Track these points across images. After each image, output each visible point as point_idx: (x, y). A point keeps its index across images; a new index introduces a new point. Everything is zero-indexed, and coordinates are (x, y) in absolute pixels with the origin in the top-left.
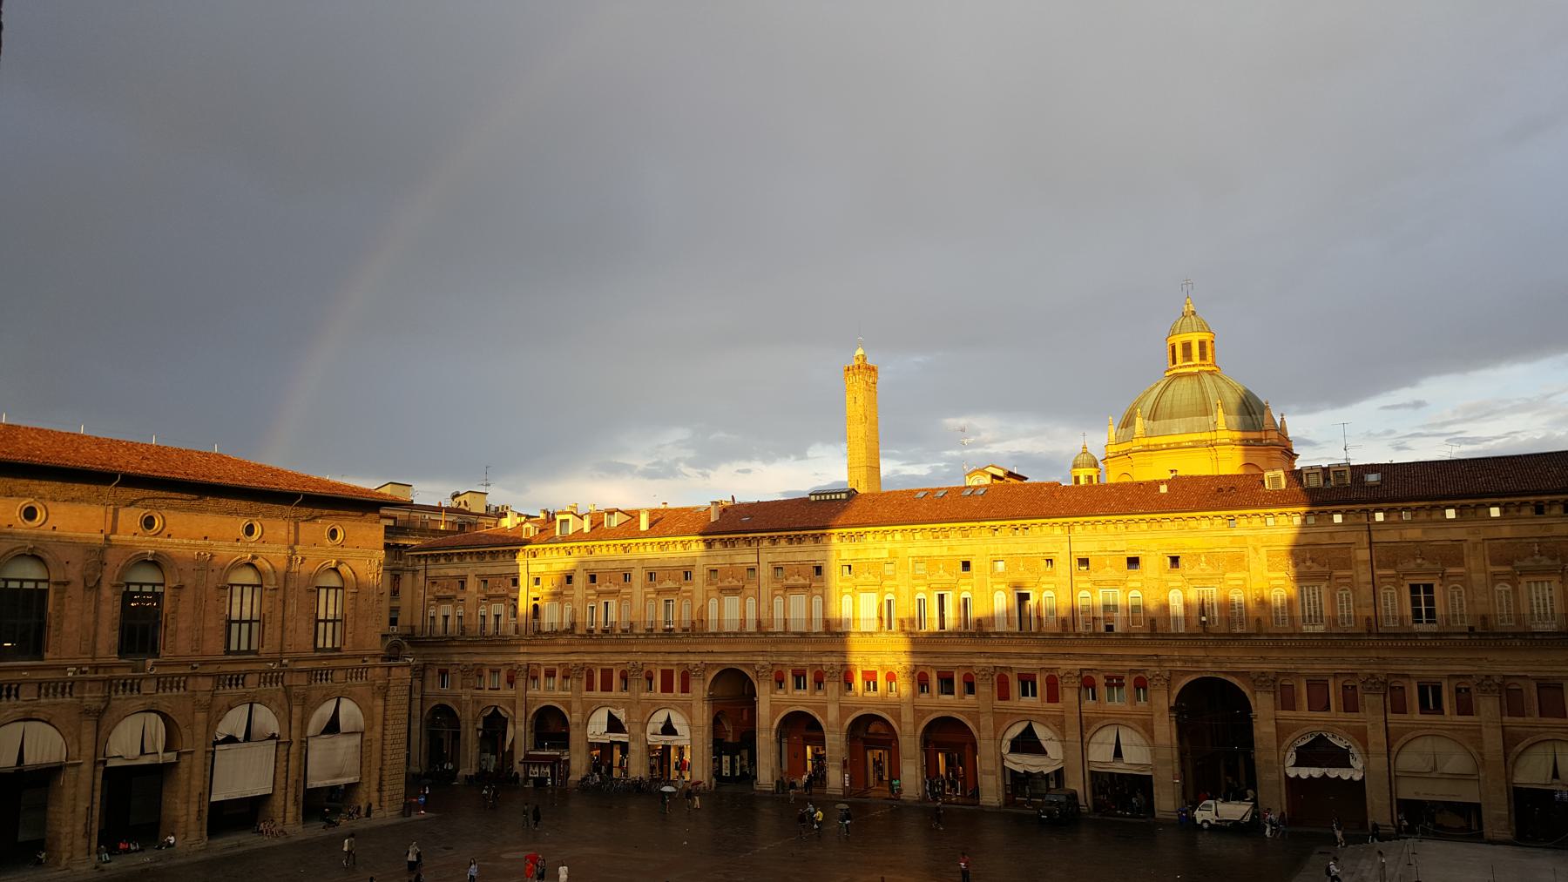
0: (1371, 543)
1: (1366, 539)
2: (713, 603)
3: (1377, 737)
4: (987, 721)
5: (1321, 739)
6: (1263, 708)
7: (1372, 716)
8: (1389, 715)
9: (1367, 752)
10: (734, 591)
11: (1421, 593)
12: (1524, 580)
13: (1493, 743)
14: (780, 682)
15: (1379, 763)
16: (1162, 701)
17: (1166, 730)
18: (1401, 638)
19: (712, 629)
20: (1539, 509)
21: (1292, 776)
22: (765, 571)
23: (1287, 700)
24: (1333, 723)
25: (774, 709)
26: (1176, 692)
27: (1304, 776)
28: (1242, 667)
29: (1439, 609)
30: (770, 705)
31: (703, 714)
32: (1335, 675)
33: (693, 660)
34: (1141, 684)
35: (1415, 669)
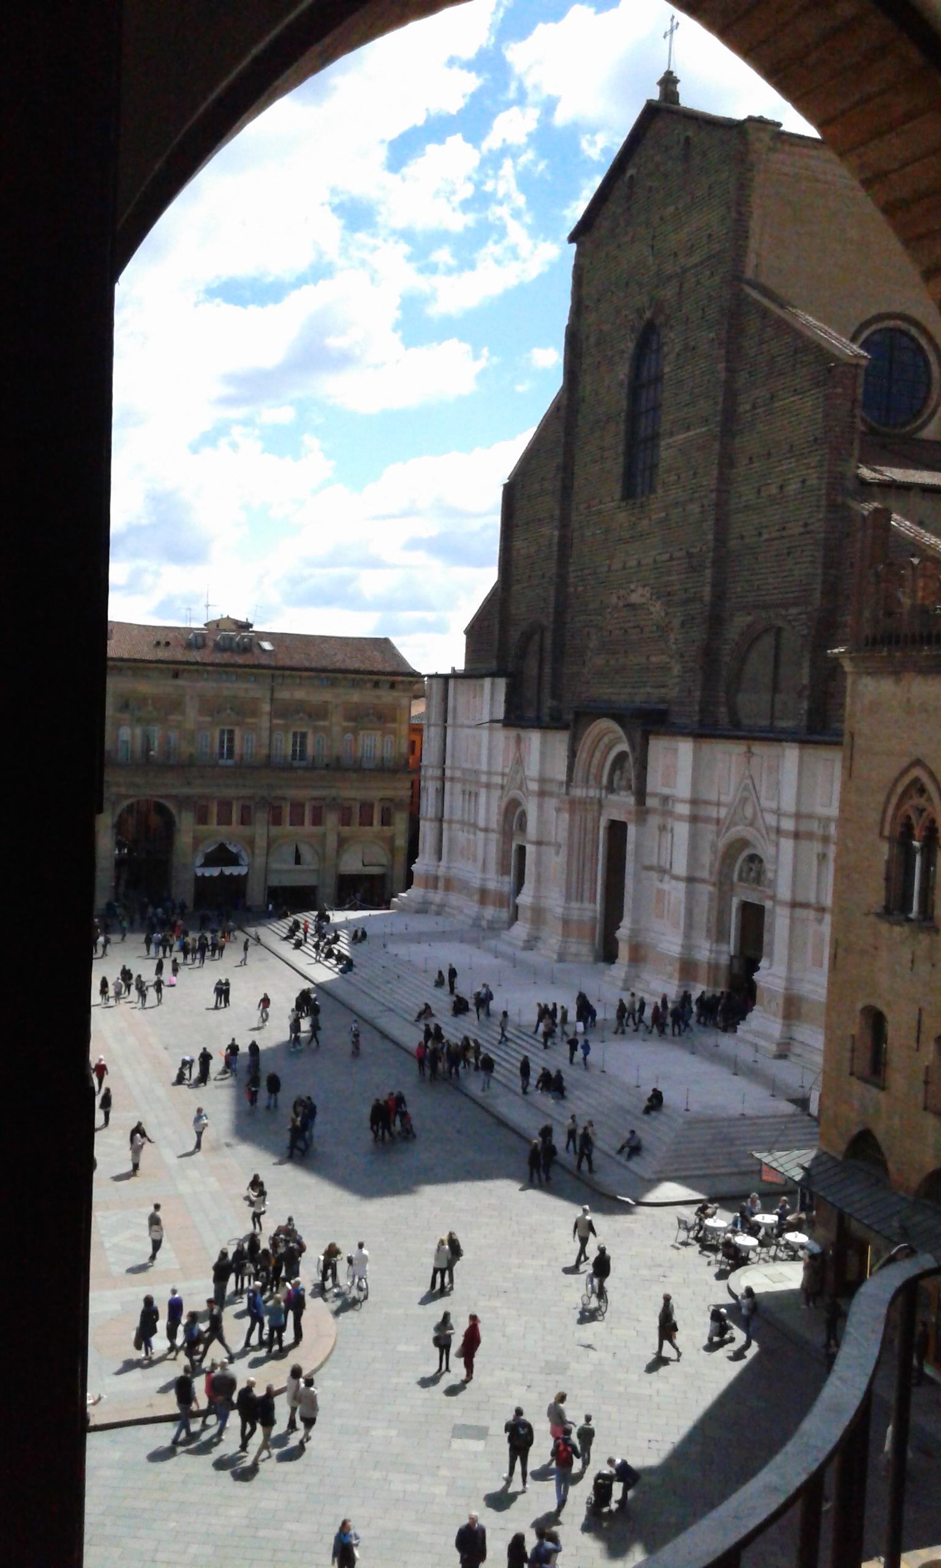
0: (272, 700)
1: (268, 695)
3: (261, 843)
5: (222, 847)
7: (260, 830)
8: (271, 827)
9: (253, 852)
12: (361, 733)
13: (332, 841)
15: (260, 861)
20: (376, 685)
21: (199, 874)
23: (202, 819)
24: (230, 834)
26: (118, 811)
27: (207, 874)
28: (174, 792)
29: (310, 750)
32: (238, 798)
35: (293, 793)
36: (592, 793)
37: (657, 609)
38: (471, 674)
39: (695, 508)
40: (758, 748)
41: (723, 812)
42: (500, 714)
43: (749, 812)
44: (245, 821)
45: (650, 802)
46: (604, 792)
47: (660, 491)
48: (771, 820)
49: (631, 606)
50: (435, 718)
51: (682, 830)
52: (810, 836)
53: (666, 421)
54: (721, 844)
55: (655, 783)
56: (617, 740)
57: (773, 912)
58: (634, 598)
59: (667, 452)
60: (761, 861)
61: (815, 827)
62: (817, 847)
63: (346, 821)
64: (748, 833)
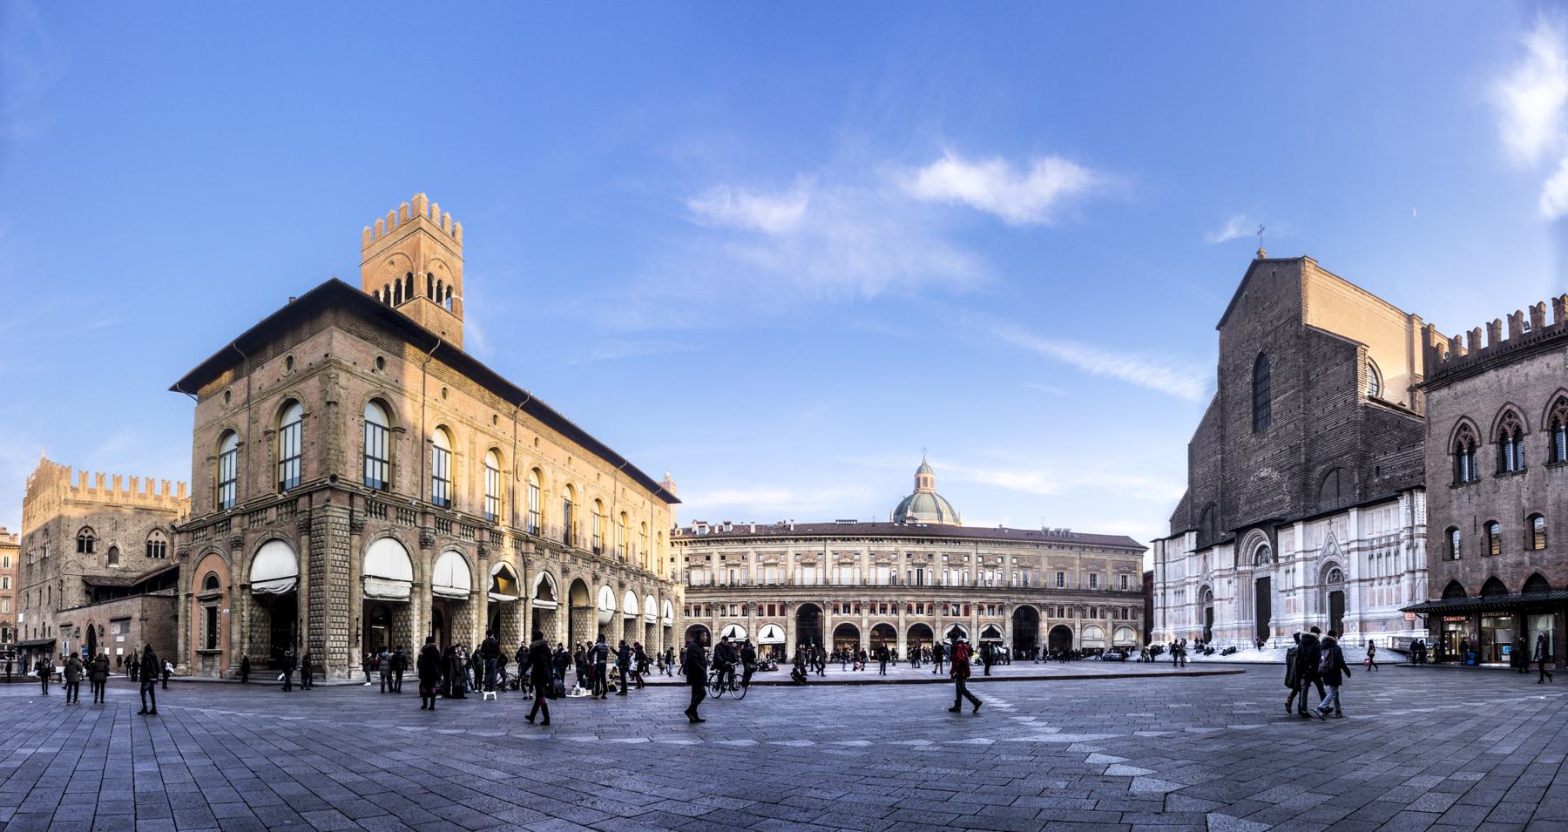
2: (798, 572)
3: (1078, 626)
4: (938, 624)
6: (1044, 615)
7: (1077, 621)
10: (812, 565)
11: (1093, 577)
14: (836, 610)
16: (1009, 614)
17: (1009, 625)
18: (1088, 593)
19: (798, 583)
22: (829, 555)
23: (1051, 615)
25: (833, 622)
30: (830, 621)
31: (792, 625)
33: (787, 599)
34: (1001, 609)
38: (1176, 536)
42: (1194, 547)
43: (1332, 549)
44: (1070, 616)
45: (1281, 561)
48: (1344, 548)
50: (1160, 560)
51: (1300, 566)
52: (1364, 549)
55: (1282, 552)
56: (1262, 539)
61: (1366, 544)
62: (1368, 553)
63: (1116, 617)
64: (1334, 558)
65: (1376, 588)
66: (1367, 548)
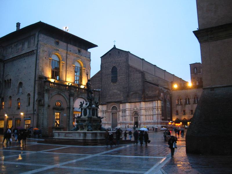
36: (110, 111)
37: (119, 92)
39: (124, 83)
40: (136, 103)
41: (132, 109)
43: (135, 109)
45: (121, 110)
46: (111, 111)
47: (118, 81)
49: (115, 92)
53: (118, 75)
54: (132, 112)
57: (140, 117)
58: (114, 91)
59: (119, 78)
60: (137, 113)
65: (147, 117)
66: (146, 109)
